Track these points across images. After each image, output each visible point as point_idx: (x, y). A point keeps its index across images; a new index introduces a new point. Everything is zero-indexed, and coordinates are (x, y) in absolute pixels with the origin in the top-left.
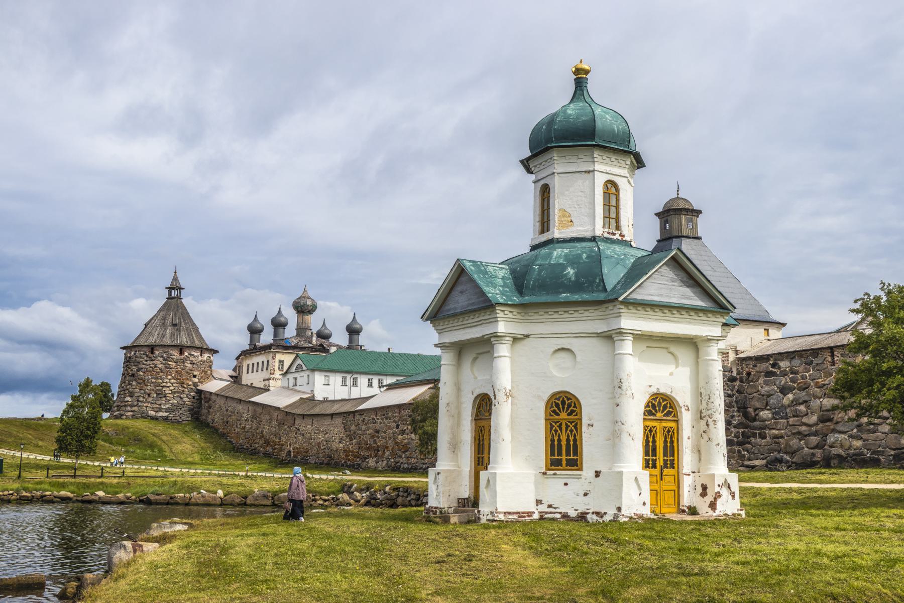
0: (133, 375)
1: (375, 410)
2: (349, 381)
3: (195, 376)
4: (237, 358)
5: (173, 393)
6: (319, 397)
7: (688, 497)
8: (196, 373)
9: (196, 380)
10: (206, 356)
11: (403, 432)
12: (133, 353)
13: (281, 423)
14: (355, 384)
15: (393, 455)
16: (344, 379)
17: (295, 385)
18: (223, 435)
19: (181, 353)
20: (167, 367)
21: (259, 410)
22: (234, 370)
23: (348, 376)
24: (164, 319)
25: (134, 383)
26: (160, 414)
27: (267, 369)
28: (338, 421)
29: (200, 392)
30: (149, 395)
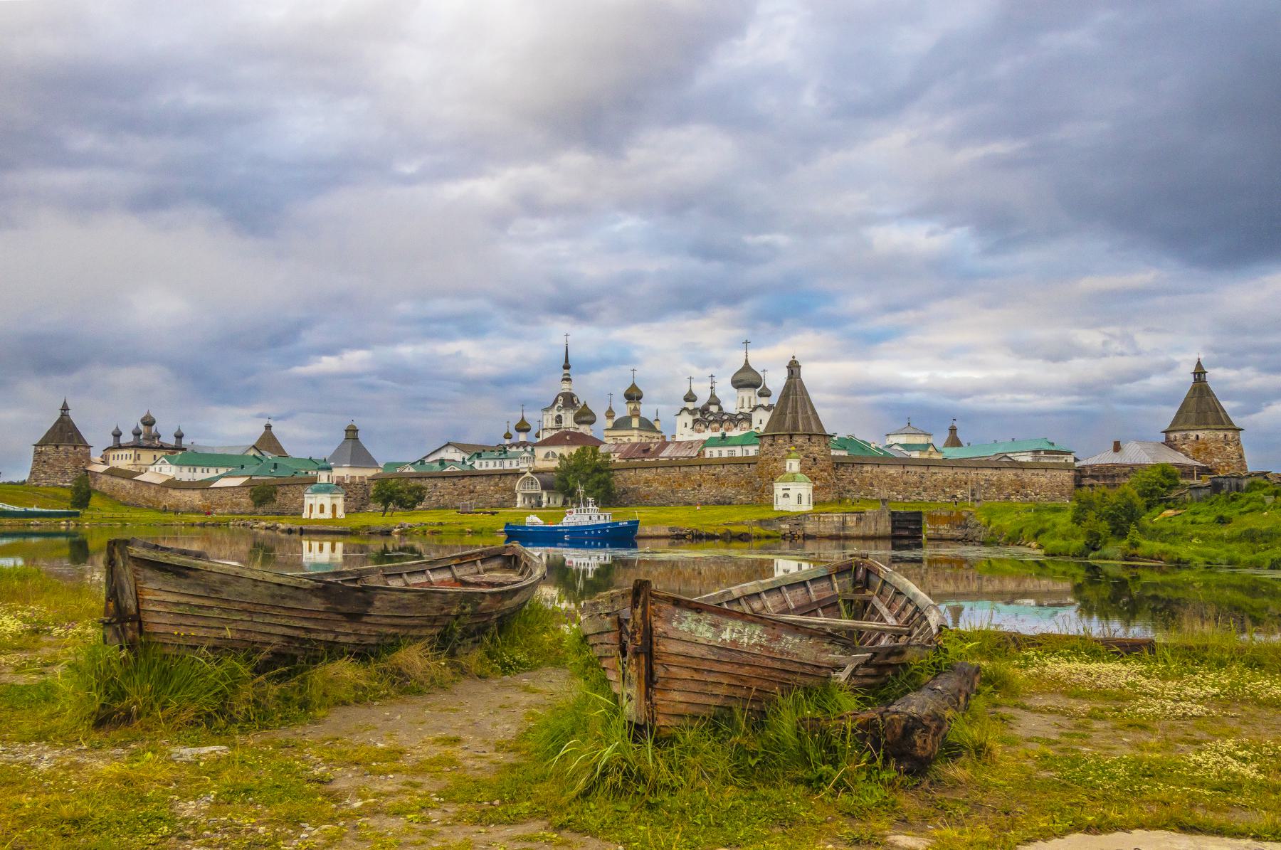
1: (220, 488)
2: (192, 470)
6: (178, 479)
11: (236, 498)
13: (157, 492)
14: (195, 471)
15: (231, 507)
17: (160, 470)
18: (111, 497)
19: (75, 449)
20: (67, 457)
21: (140, 484)
22: (102, 457)
28: (198, 492)
29: (87, 471)
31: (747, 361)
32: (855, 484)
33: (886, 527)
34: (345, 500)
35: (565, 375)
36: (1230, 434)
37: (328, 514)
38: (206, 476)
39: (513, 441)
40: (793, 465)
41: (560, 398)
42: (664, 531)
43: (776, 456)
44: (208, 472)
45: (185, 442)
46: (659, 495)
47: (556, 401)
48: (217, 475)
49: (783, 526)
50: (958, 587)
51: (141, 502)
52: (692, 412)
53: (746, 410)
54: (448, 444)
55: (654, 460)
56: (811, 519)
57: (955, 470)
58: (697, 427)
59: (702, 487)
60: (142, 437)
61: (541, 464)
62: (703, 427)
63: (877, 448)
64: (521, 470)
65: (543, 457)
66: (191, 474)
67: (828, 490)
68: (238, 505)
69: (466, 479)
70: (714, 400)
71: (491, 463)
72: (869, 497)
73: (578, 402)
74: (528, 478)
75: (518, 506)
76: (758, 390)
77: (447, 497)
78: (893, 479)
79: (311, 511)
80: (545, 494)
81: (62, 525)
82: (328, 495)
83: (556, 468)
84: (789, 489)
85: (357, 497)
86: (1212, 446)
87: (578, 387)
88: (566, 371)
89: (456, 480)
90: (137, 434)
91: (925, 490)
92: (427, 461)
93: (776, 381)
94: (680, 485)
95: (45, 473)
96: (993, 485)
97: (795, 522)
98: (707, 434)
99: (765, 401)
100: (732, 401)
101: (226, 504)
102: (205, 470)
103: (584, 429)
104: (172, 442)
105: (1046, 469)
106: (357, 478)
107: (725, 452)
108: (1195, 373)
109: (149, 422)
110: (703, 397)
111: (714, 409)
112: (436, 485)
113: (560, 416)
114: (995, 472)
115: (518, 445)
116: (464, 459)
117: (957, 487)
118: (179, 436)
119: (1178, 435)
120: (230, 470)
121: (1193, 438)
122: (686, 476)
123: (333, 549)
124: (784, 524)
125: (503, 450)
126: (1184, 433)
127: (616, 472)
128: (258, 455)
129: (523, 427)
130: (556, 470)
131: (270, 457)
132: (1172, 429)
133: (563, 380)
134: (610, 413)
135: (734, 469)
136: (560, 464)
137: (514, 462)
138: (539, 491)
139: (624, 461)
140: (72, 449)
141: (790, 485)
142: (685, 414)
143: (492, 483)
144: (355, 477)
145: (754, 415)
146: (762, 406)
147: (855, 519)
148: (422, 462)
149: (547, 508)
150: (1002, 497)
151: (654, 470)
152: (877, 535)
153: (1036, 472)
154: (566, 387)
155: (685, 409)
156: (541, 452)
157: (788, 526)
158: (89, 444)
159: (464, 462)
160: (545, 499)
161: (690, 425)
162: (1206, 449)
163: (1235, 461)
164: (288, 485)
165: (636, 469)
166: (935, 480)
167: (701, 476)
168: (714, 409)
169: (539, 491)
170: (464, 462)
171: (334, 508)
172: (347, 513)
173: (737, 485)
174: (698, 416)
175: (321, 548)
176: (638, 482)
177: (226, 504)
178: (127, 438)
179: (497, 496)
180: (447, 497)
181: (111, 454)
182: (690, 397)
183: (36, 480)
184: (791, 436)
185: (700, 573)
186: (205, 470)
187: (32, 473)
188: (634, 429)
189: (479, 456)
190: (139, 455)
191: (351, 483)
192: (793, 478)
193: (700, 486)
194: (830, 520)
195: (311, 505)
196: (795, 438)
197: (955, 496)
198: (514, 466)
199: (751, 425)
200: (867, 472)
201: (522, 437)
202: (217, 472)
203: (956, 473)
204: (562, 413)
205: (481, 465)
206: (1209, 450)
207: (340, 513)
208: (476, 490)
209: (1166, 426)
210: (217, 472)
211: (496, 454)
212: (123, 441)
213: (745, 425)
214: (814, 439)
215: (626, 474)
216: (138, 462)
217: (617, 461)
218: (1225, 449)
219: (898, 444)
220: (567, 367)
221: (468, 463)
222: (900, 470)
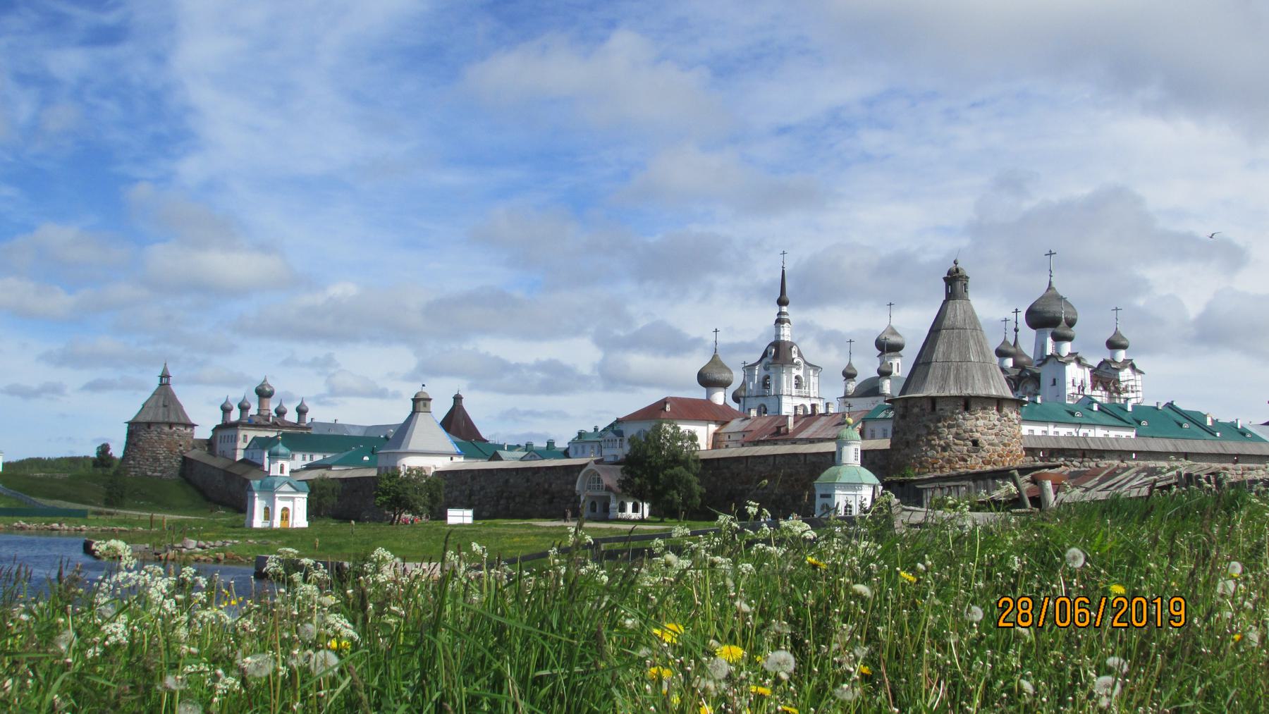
3: (181, 445)
5: (165, 458)
8: (181, 443)
9: (182, 448)
10: (189, 430)
20: (160, 439)
88: (785, 309)
112: (507, 481)
158: (193, 421)
181: (220, 433)
212: (235, 416)
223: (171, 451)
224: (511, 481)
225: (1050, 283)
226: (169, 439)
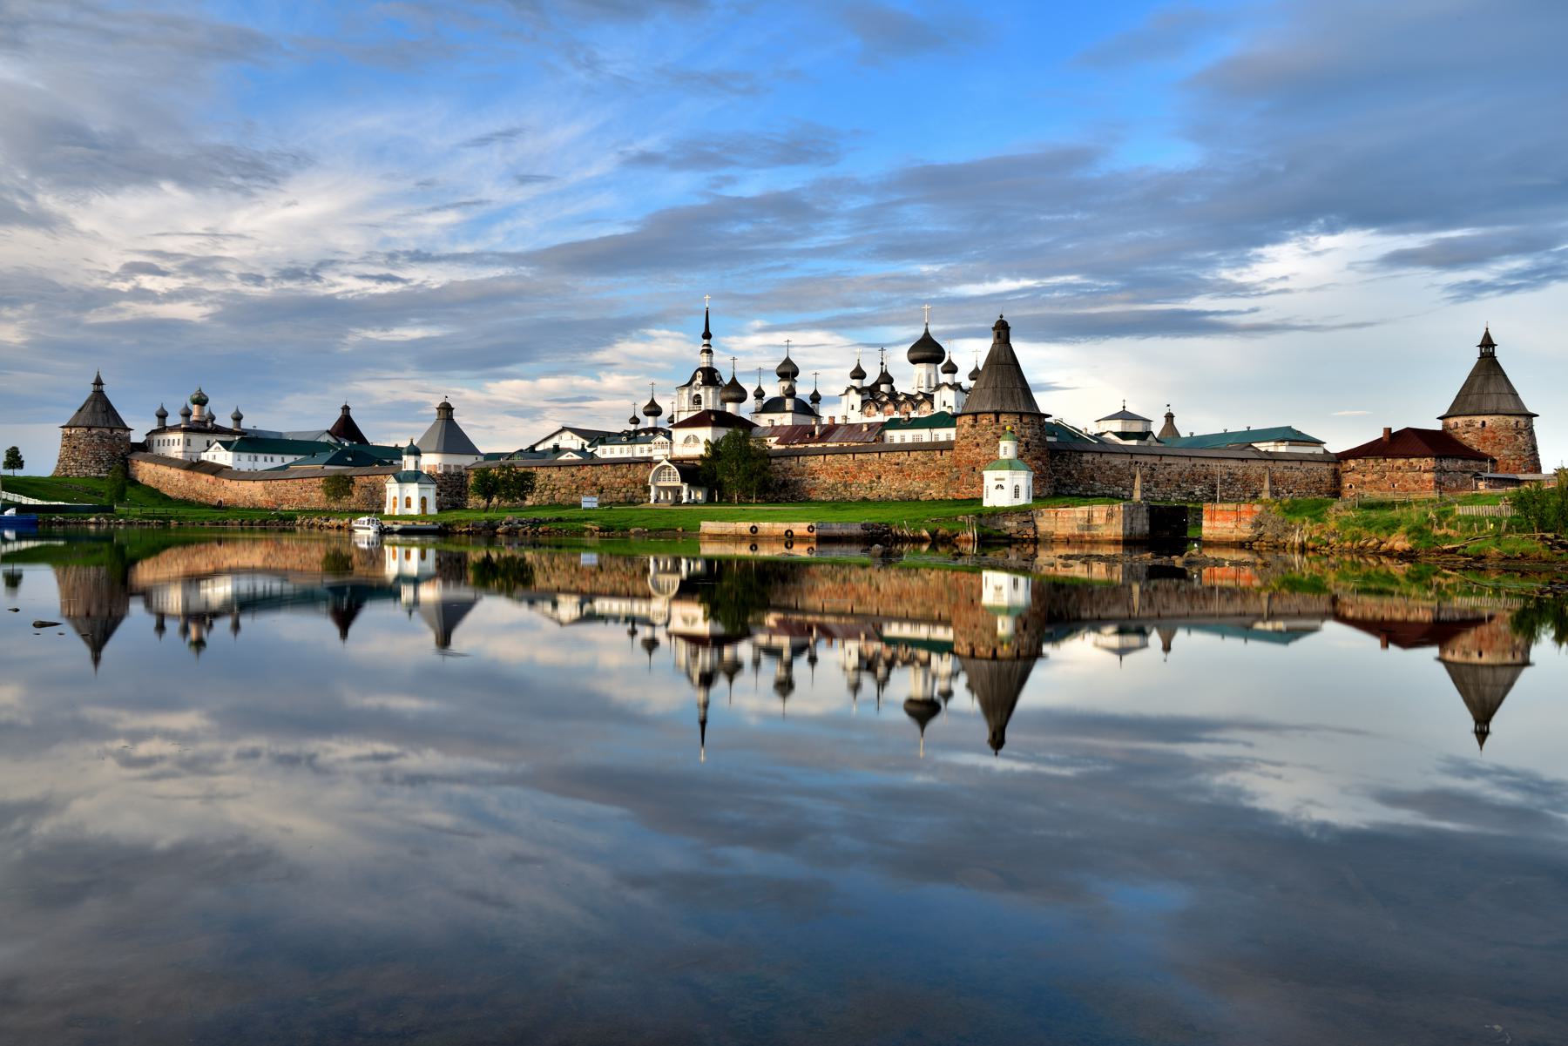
0: (75, 447)
2: (252, 459)
4: (147, 435)
6: (235, 469)
7: (428, 513)
9: (123, 451)
10: (127, 433)
12: (73, 432)
14: (256, 459)
16: (249, 457)
19: (112, 432)
20: (103, 442)
23: (252, 455)
24: (94, 407)
25: (77, 453)
26: (100, 475)
27: (178, 444)
28: (259, 484)
30: (90, 462)
31: (927, 330)
32: (1072, 476)
33: (1143, 525)
34: (438, 494)
35: (704, 345)
36: (1522, 421)
37: (415, 510)
38: (269, 465)
39: (640, 427)
40: (1007, 449)
41: (700, 373)
42: (855, 530)
43: (979, 440)
44: (272, 460)
45: (246, 424)
46: (827, 489)
47: (694, 378)
48: (284, 464)
49: (1007, 524)
50: (1193, 608)
51: (192, 496)
52: (859, 391)
53: (923, 390)
54: (564, 429)
55: (820, 445)
56: (1046, 515)
57: (1194, 461)
58: (867, 410)
59: (882, 480)
60: (192, 418)
61: (681, 451)
62: (873, 410)
63: (1089, 436)
64: (655, 458)
65: (682, 442)
66: (250, 463)
67: (1042, 483)
68: (308, 500)
69: (587, 469)
70: (886, 378)
71: (617, 448)
72: (1089, 493)
73: (721, 379)
74: (665, 467)
75: (652, 501)
76: (940, 366)
77: (563, 491)
78: (1119, 471)
79: (395, 505)
80: (685, 487)
81: (91, 523)
82: (416, 485)
83: (701, 456)
84: (1003, 479)
85: (451, 488)
86: (1501, 434)
87: (721, 362)
88: (706, 342)
89: (574, 470)
90: (187, 414)
91: (1157, 485)
92: (537, 449)
93: (970, 353)
94: (855, 477)
95: (76, 461)
96: (1238, 480)
97: (1025, 519)
98: (880, 418)
99: (945, 378)
100: (911, 379)
101: (294, 500)
102: (269, 459)
103: (730, 408)
104: (228, 423)
105: (1301, 461)
106: (452, 468)
107: (909, 436)
108: (1481, 346)
109: (201, 401)
110: (871, 379)
111: (884, 388)
112: (549, 476)
113: (698, 396)
114: (1241, 464)
115: (646, 431)
116: (583, 445)
117: (1196, 482)
118: (238, 418)
119: (1460, 421)
120: (299, 458)
121: (1479, 425)
122: (861, 465)
123: (423, 556)
124: (1010, 521)
125: (632, 438)
126: (1467, 419)
127: (773, 461)
128: (332, 440)
129: (653, 410)
130: (701, 458)
131: (346, 444)
132: (1453, 414)
133: (703, 351)
134: (759, 394)
135: (920, 455)
136: (707, 450)
137: (646, 447)
138: (678, 483)
139: (783, 447)
140: (108, 432)
141: (1005, 474)
142: (853, 392)
143: (619, 473)
144: (449, 466)
145: (937, 395)
146: (947, 384)
147: (1104, 514)
148: (532, 448)
149: (687, 503)
150: (1248, 495)
151: (822, 457)
152: (1133, 538)
153: (1289, 464)
154: (704, 361)
155: (854, 387)
156: (679, 435)
157: (1015, 524)
158: (129, 427)
159: (583, 450)
160: (685, 494)
161: (858, 406)
162: (1494, 438)
163: (1527, 454)
164: (367, 476)
165: (798, 457)
166: (1169, 474)
167: (881, 465)
168: (884, 388)
169: (678, 483)
170: (583, 450)
171: (423, 501)
172: (440, 510)
173: (925, 476)
174: (867, 397)
175: (408, 555)
176: (802, 474)
177: (294, 500)
178: (174, 419)
179: (624, 490)
180: (563, 491)
181: (156, 438)
182: (859, 374)
183: (66, 470)
184: (997, 414)
185: (878, 589)
186: (269, 459)
187: (59, 461)
188: (785, 411)
189: (603, 442)
190: (189, 441)
191: (445, 473)
192: (1010, 465)
193: (879, 477)
194: (1072, 516)
195: (395, 498)
196: (1002, 418)
197: (1193, 493)
198: (645, 454)
199: (932, 407)
200: (1087, 462)
201: (650, 422)
202: (283, 461)
203: (1195, 465)
204: (701, 392)
205: (604, 452)
206: (1497, 441)
207: (432, 509)
208: (598, 483)
209: (1444, 412)
210: (283, 461)
211: (624, 439)
213: (926, 407)
214: (1025, 420)
215: (786, 463)
216: (189, 449)
217: (775, 447)
218: (1516, 439)
219: (1111, 432)
220: (707, 335)
221: (589, 450)
222: (1127, 459)
223: (113, 454)
224: (554, 476)
225: (927, 330)
226: (111, 442)
